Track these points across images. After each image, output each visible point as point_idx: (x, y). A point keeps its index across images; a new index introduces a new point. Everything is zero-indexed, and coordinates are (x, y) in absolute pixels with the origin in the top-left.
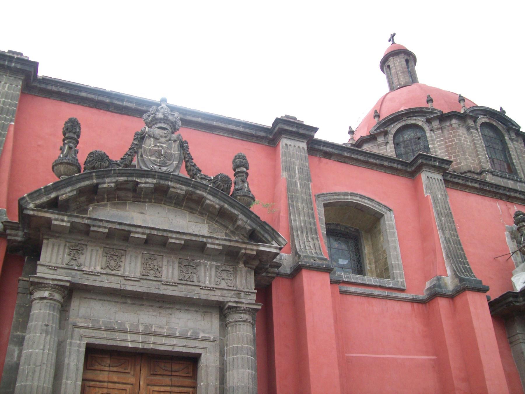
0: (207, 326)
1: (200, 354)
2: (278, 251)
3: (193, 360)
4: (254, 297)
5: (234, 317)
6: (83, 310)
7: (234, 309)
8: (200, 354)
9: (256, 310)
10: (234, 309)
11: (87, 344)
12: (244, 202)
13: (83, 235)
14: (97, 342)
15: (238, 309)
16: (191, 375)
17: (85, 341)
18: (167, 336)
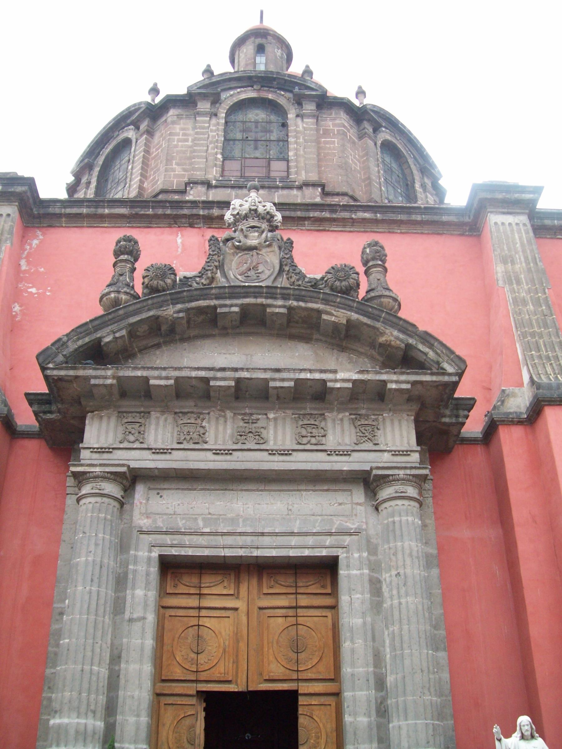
0: (345, 509)
1: (337, 557)
2: (455, 379)
3: (326, 569)
4: (416, 457)
5: (386, 492)
6: (156, 508)
7: (384, 480)
8: (337, 557)
9: (424, 478)
10: (384, 480)
11: (160, 556)
12: (382, 307)
13: (136, 399)
14: (174, 552)
15: (391, 478)
16: (329, 591)
17: (155, 554)
18: (299, 534)
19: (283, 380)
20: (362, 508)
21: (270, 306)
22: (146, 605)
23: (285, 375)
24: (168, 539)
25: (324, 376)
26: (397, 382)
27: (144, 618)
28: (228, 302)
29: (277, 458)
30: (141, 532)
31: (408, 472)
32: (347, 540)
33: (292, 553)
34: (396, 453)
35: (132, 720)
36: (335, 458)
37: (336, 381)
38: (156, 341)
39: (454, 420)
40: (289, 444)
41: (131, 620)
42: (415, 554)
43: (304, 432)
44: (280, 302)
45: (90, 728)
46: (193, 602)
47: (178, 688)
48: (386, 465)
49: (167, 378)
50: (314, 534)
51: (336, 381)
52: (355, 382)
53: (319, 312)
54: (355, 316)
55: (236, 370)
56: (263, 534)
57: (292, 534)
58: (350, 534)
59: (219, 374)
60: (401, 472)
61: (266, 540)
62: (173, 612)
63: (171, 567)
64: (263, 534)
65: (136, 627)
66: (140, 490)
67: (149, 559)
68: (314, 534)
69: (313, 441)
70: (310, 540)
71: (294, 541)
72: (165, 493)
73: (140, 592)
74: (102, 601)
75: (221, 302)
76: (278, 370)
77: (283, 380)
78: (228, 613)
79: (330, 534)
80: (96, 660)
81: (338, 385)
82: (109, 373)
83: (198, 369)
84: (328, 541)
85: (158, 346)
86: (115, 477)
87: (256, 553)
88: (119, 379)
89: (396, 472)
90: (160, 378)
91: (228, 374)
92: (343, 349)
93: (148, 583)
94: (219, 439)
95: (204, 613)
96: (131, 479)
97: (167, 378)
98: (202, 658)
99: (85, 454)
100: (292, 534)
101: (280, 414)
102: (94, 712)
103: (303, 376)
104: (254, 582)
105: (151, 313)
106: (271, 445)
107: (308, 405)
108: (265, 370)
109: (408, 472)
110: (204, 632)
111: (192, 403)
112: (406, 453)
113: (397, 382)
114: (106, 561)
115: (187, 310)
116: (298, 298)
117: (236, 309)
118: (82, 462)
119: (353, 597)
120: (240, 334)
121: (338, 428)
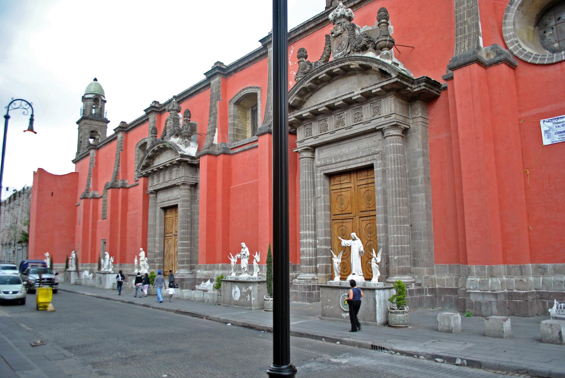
19: (338, 101)
20: (381, 142)
21: (334, 69)
22: (321, 192)
23: (339, 99)
24: (325, 168)
25: (350, 95)
26: (375, 89)
27: (321, 196)
28: (321, 73)
29: (348, 130)
30: (318, 167)
31: (388, 125)
32: (376, 156)
33: (359, 165)
34: (386, 117)
35: (320, 230)
36: (366, 125)
37: (354, 96)
38: (310, 94)
39: (419, 89)
40: (352, 124)
41: (317, 198)
42: (393, 159)
43: (356, 117)
44: (336, 67)
45: (308, 234)
46: (338, 187)
47: (337, 217)
48: (381, 124)
49: (307, 113)
50: (365, 156)
51: (354, 96)
52: (361, 94)
53: (349, 65)
54: (361, 62)
55: (324, 103)
56: (350, 160)
57: (358, 158)
58: (376, 154)
59: (320, 106)
60: (386, 126)
61: (351, 162)
62: (334, 191)
63: (330, 176)
64: (350, 160)
65: (319, 200)
66: (317, 150)
67: (321, 176)
68: (365, 156)
69: (359, 119)
70: (364, 159)
71: (359, 160)
72: (323, 150)
73: (319, 188)
74: (307, 194)
75: (319, 74)
76: (336, 98)
77: (338, 101)
78: (348, 189)
79: (370, 155)
80: (307, 213)
81: (356, 97)
82: (292, 116)
83: (314, 106)
84: (370, 158)
85: (311, 95)
86: (306, 150)
87: (349, 167)
88: (296, 117)
89: (384, 126)
90: (305, 113)
91: (323, 105)
92: (367, 74)
93: (321, 184)
94: (332, 127)
95: (342, 190)
96: (313, 148)
97: (307, 113)
98: (343, 206)
99: (298, 144)
100: (358, 158)
101: (348, 111)
102: (309, 229)
103: (346, 97)
104: (355, 176)
105: (301, 87)
106: (346, 126)
107: (355, 105)
108: (332, 100)
109: (388, 125)
110: (343, 197)
111: (321, 116)
112: (389, 116)
113: (375, 89)
114: (307, 180)
115: (311, 81)
116: (341, 62)
117: (324, 75)
118: (298, 147)
119: (378, 179)
120: (334, 81)
121: (366, 111)
